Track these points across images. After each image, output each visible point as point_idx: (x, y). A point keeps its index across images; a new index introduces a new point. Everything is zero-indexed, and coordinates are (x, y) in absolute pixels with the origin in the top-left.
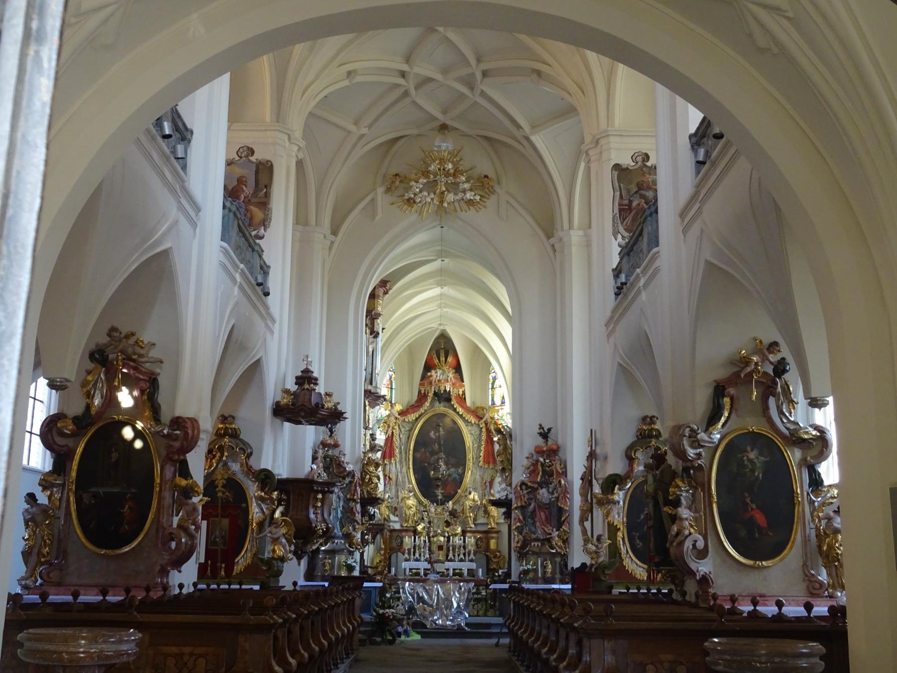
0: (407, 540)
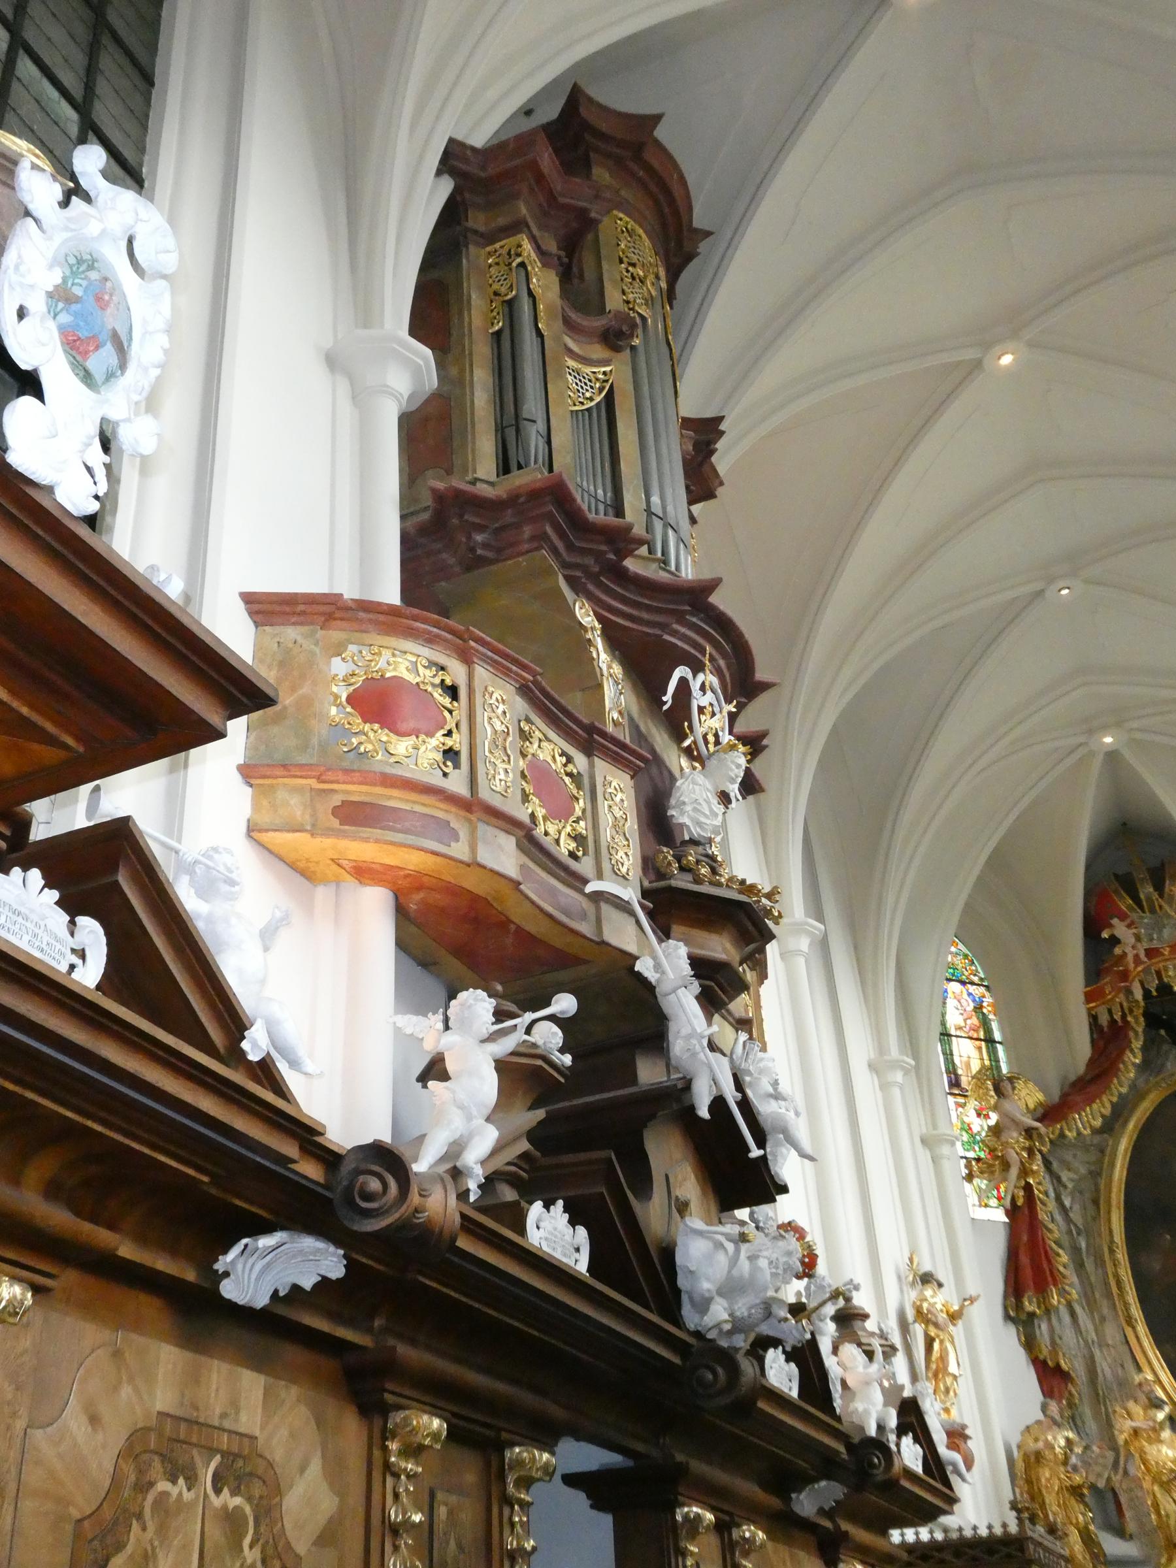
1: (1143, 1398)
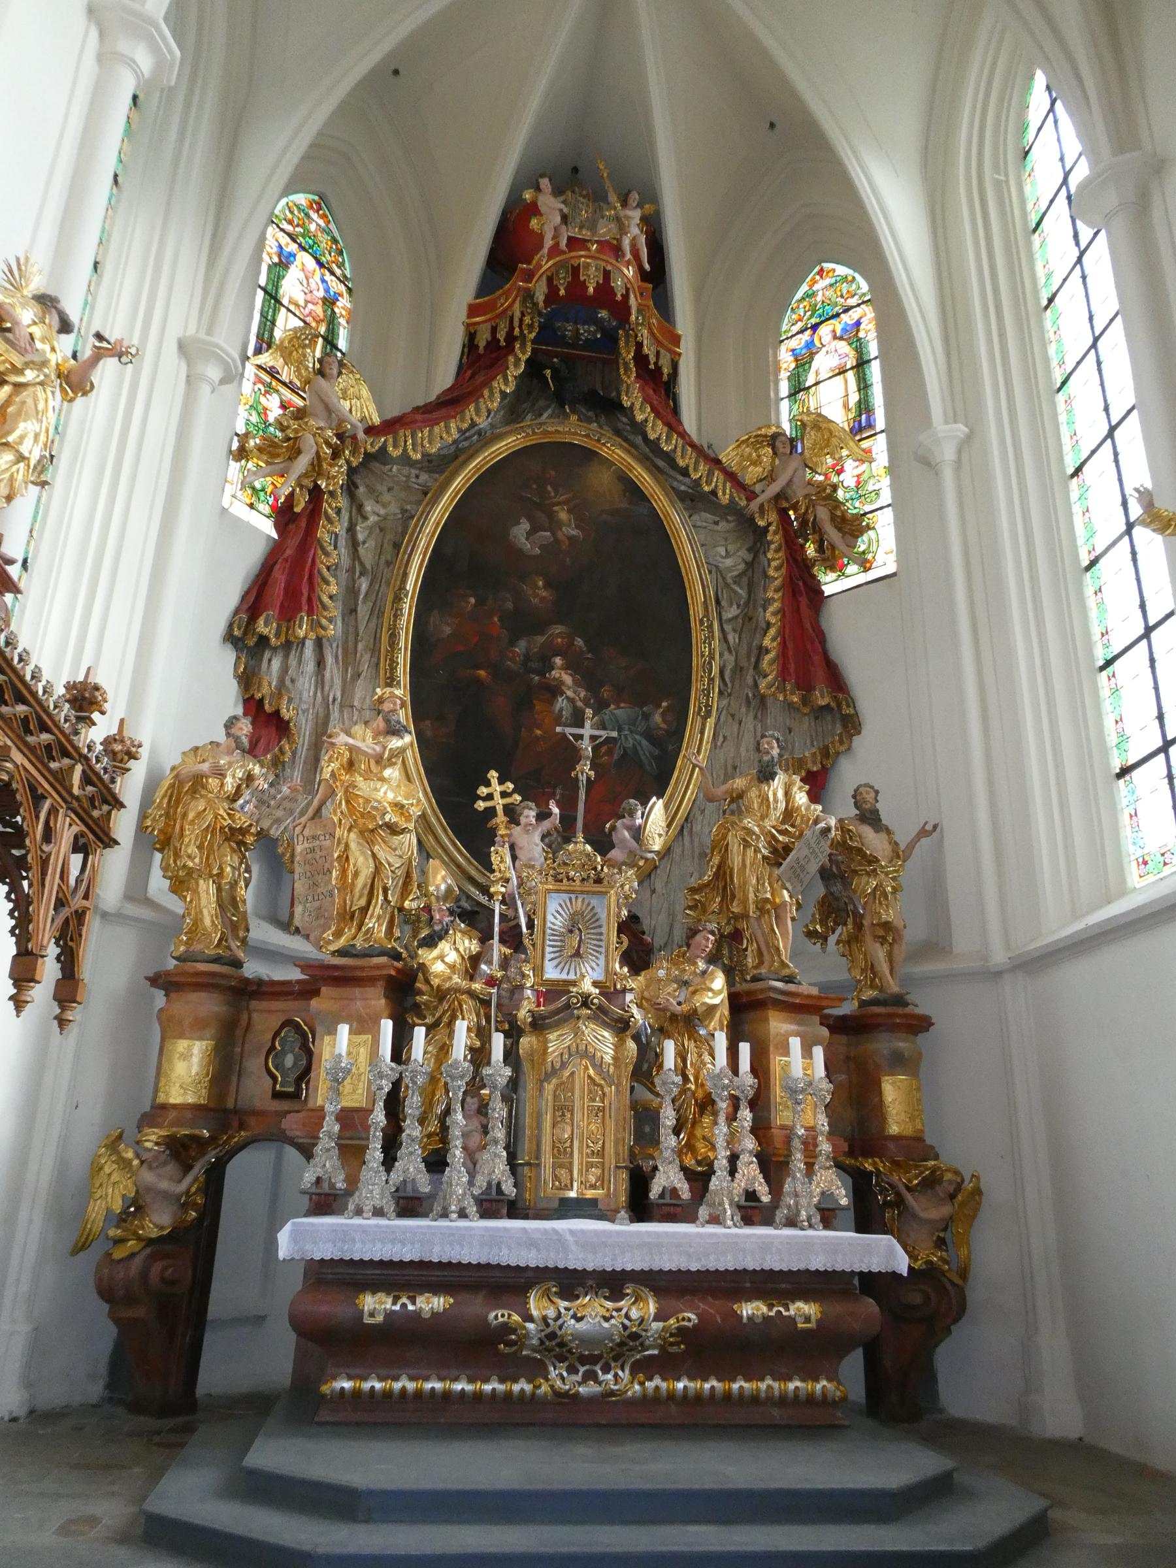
0: (340, 1043)
1: (380, 722)
